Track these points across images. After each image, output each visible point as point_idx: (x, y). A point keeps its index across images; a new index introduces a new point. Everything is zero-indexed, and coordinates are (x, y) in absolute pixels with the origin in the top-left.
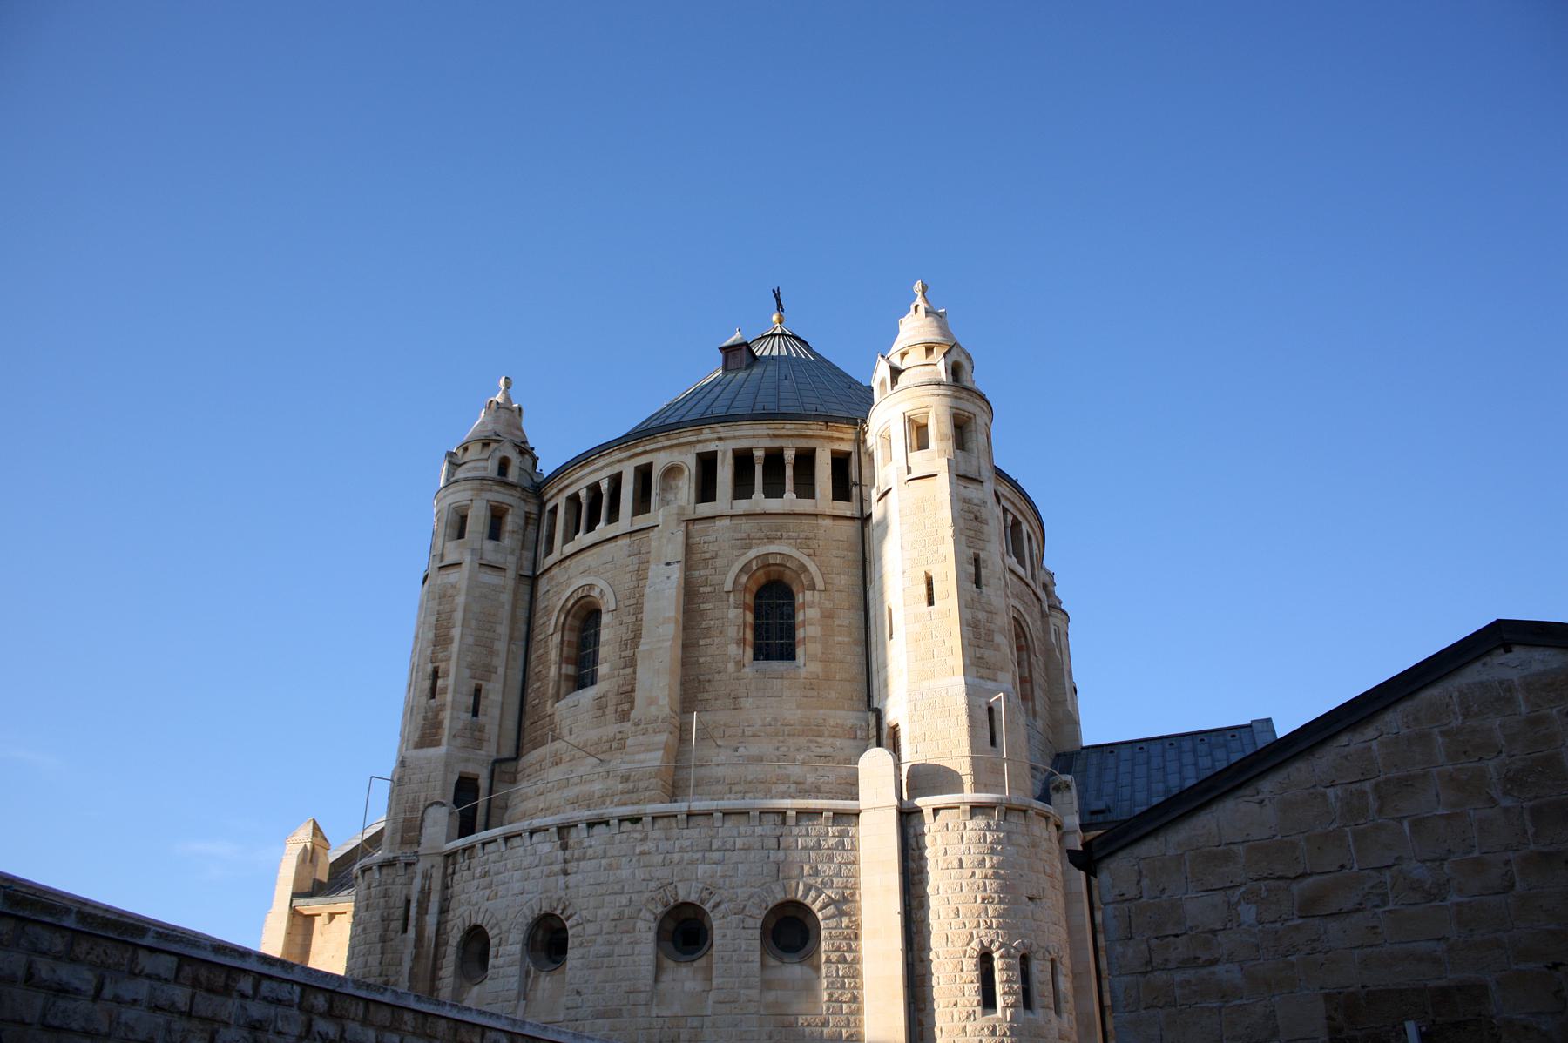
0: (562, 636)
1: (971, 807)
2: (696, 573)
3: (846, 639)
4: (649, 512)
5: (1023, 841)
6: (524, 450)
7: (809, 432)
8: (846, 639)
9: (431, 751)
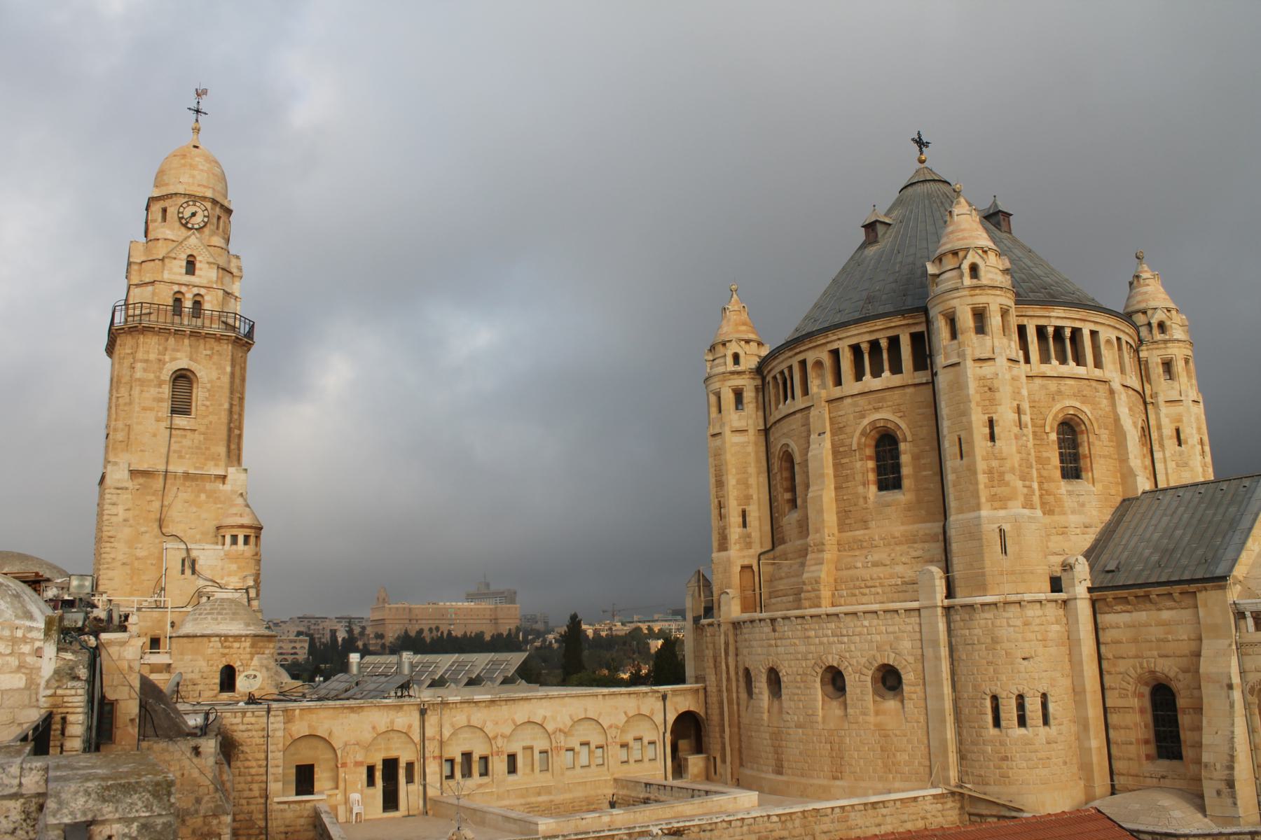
0: (781, 474)
2: (836, 438)
3: (930, 473)
5: (1019, 623)
7: (893, 324)
8: (930, 473)
9: (723, 554)
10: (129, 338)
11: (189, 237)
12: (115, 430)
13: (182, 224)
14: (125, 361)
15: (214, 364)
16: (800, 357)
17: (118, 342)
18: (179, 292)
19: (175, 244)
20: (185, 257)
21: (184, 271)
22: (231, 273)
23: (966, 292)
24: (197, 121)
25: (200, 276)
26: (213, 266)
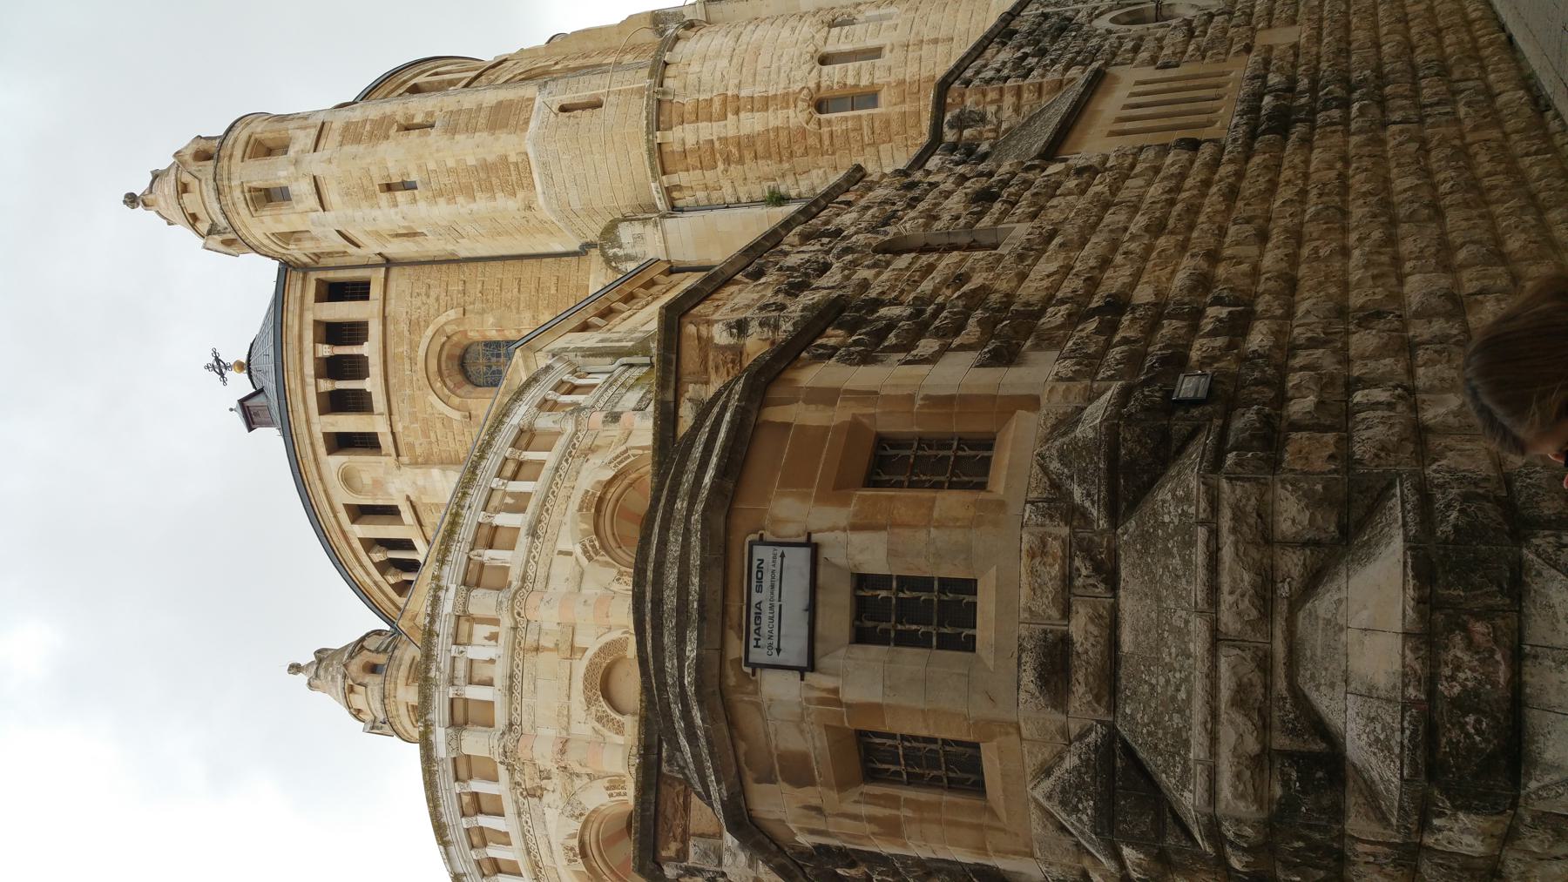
1: (658, 129)
4: (396, 507)
6: (360, 645)
16: (344, 517)
23: (225, 162)
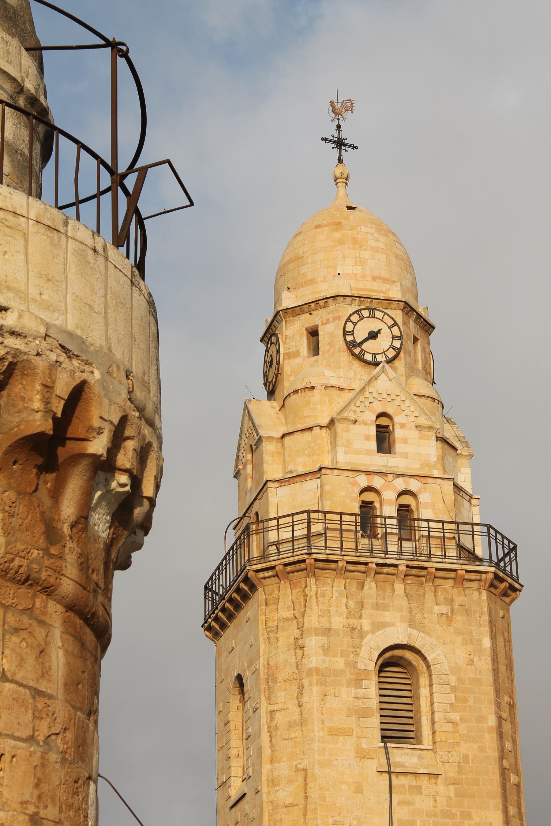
10: (285, 585)
11: (376, 378)
12: (273, 782)
13: (353, 354)
14: (281, 634)
15: (458, 632)
17: (260, 595)
18: (369, 489)
19: (349, 396)
20: (374, 418)
21: (373, 445)
22: (455, 449)
24: (340, 160)
25: (405, 456)
26: (426, 432)
